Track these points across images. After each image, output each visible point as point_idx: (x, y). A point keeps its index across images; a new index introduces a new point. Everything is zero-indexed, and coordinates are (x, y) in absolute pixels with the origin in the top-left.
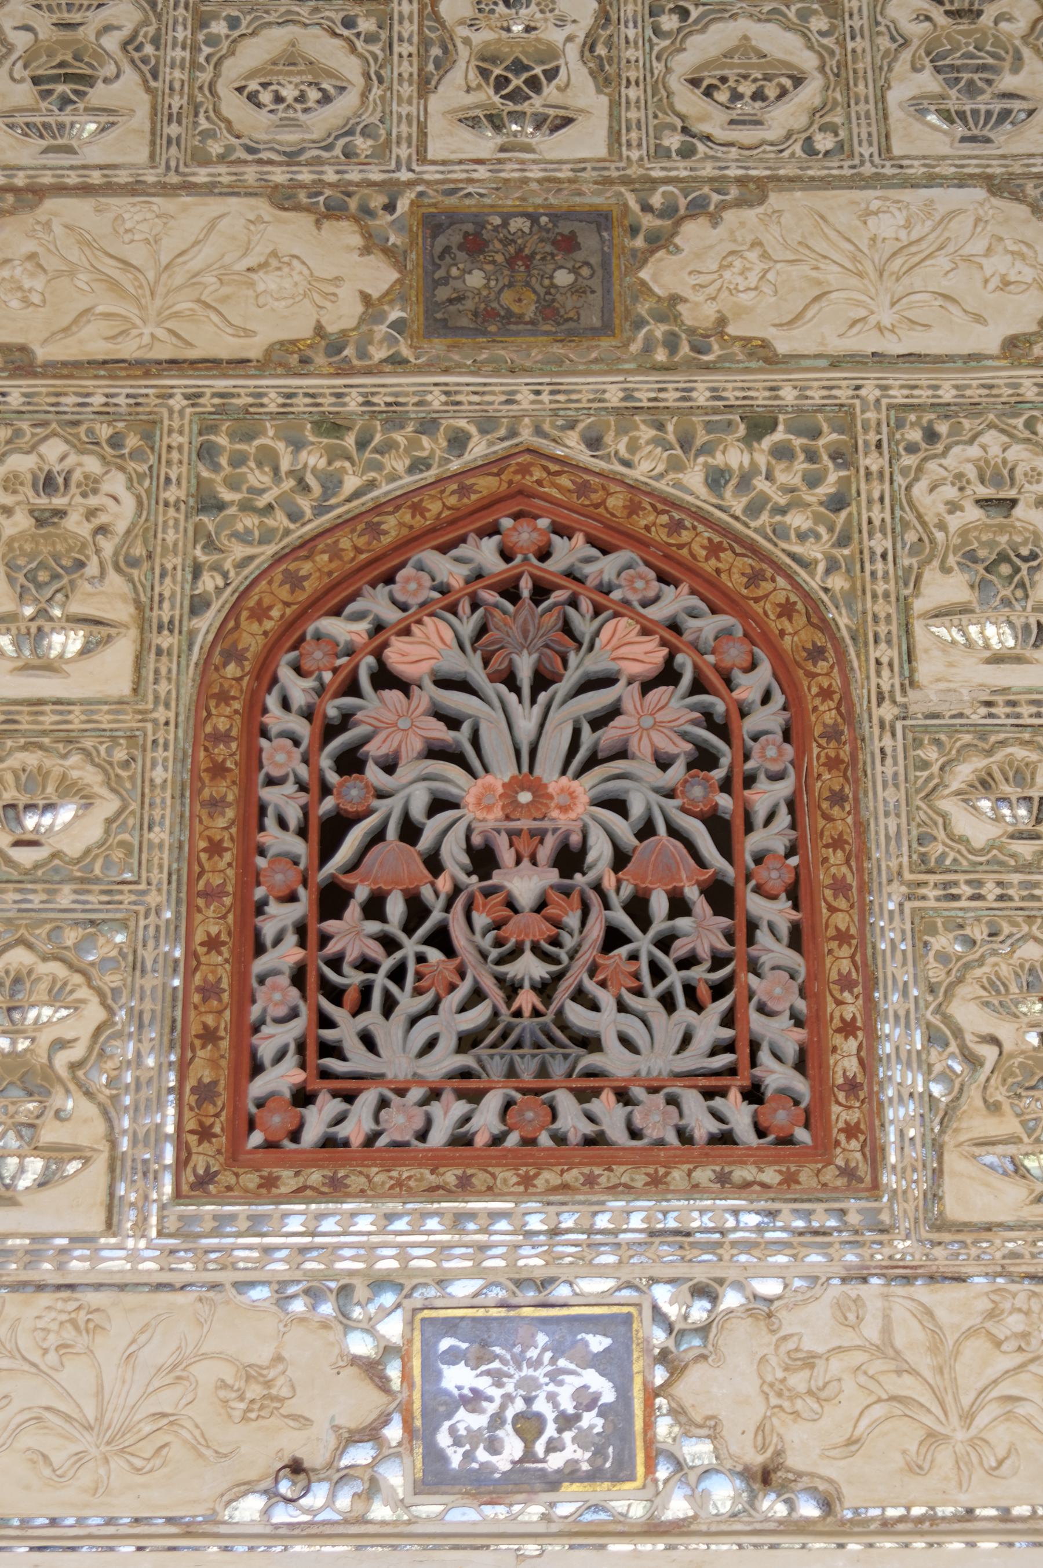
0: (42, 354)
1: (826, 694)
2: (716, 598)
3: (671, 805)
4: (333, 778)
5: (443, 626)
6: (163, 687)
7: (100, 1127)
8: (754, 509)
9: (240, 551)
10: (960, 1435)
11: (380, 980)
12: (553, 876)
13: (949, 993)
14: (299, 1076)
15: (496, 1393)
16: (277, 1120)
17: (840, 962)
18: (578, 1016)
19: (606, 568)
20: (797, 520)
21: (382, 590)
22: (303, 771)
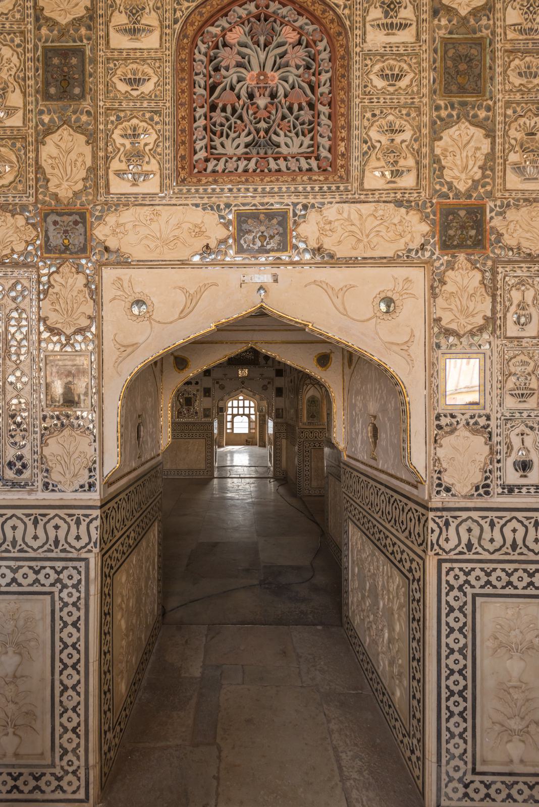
1: (341, 46)
2: (314, 19)
3: (299, 79)
4: (212, 73)
5: (240, 28)
6: (167, 45)
7: (158, 166)
10: (366, 240)
11: (225, 129)
12: (269, 100)
13: (369, 128)
14: (206, 154)
16: (201, 166)
17: (342, 122)
18: (274, 138)
19: (284, 11)
21: (224, 18)
22: (205, 71)
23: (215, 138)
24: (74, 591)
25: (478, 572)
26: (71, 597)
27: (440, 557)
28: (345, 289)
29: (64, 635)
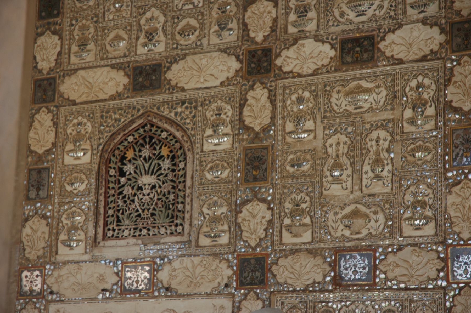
0: (78, 101)
8: (181, 119)
9: (106, 135)
15: (133, 277)
20: (188, 121)
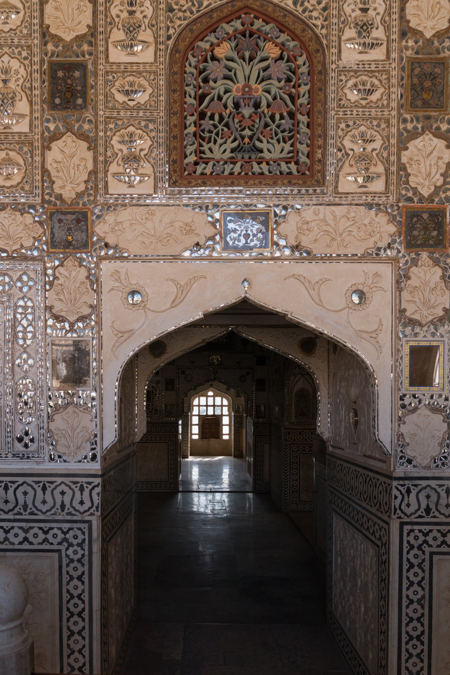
1: (319, 62)
2: (294, 36)
3: (281, 91)
4: (202, 84)
5: (228, 44)
6: (161, 59)
7: (152, 169)
8: (304, 11)
9: (178, 22)
10: (339, 239)
11: (213, 135)
12: (253, 110)
13: (343, 139)
14: (195, 158)
16: (191, 169)
17: (319, 131)
18: (258, 144)
19: (267, 28)
20: (315, 14)
21: (213, 34)
22: (195, 82)
23: (204, 143)
24: (79, 549)
25: (435, 533)
26: (77, 554)
27: (402, 520)
28: (321, 282)
29: (71, 587)
